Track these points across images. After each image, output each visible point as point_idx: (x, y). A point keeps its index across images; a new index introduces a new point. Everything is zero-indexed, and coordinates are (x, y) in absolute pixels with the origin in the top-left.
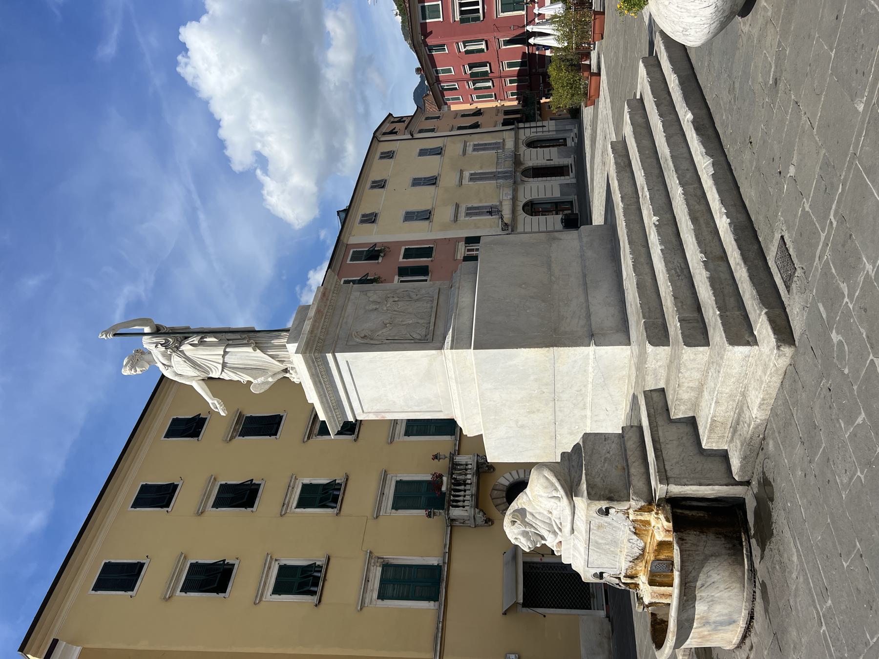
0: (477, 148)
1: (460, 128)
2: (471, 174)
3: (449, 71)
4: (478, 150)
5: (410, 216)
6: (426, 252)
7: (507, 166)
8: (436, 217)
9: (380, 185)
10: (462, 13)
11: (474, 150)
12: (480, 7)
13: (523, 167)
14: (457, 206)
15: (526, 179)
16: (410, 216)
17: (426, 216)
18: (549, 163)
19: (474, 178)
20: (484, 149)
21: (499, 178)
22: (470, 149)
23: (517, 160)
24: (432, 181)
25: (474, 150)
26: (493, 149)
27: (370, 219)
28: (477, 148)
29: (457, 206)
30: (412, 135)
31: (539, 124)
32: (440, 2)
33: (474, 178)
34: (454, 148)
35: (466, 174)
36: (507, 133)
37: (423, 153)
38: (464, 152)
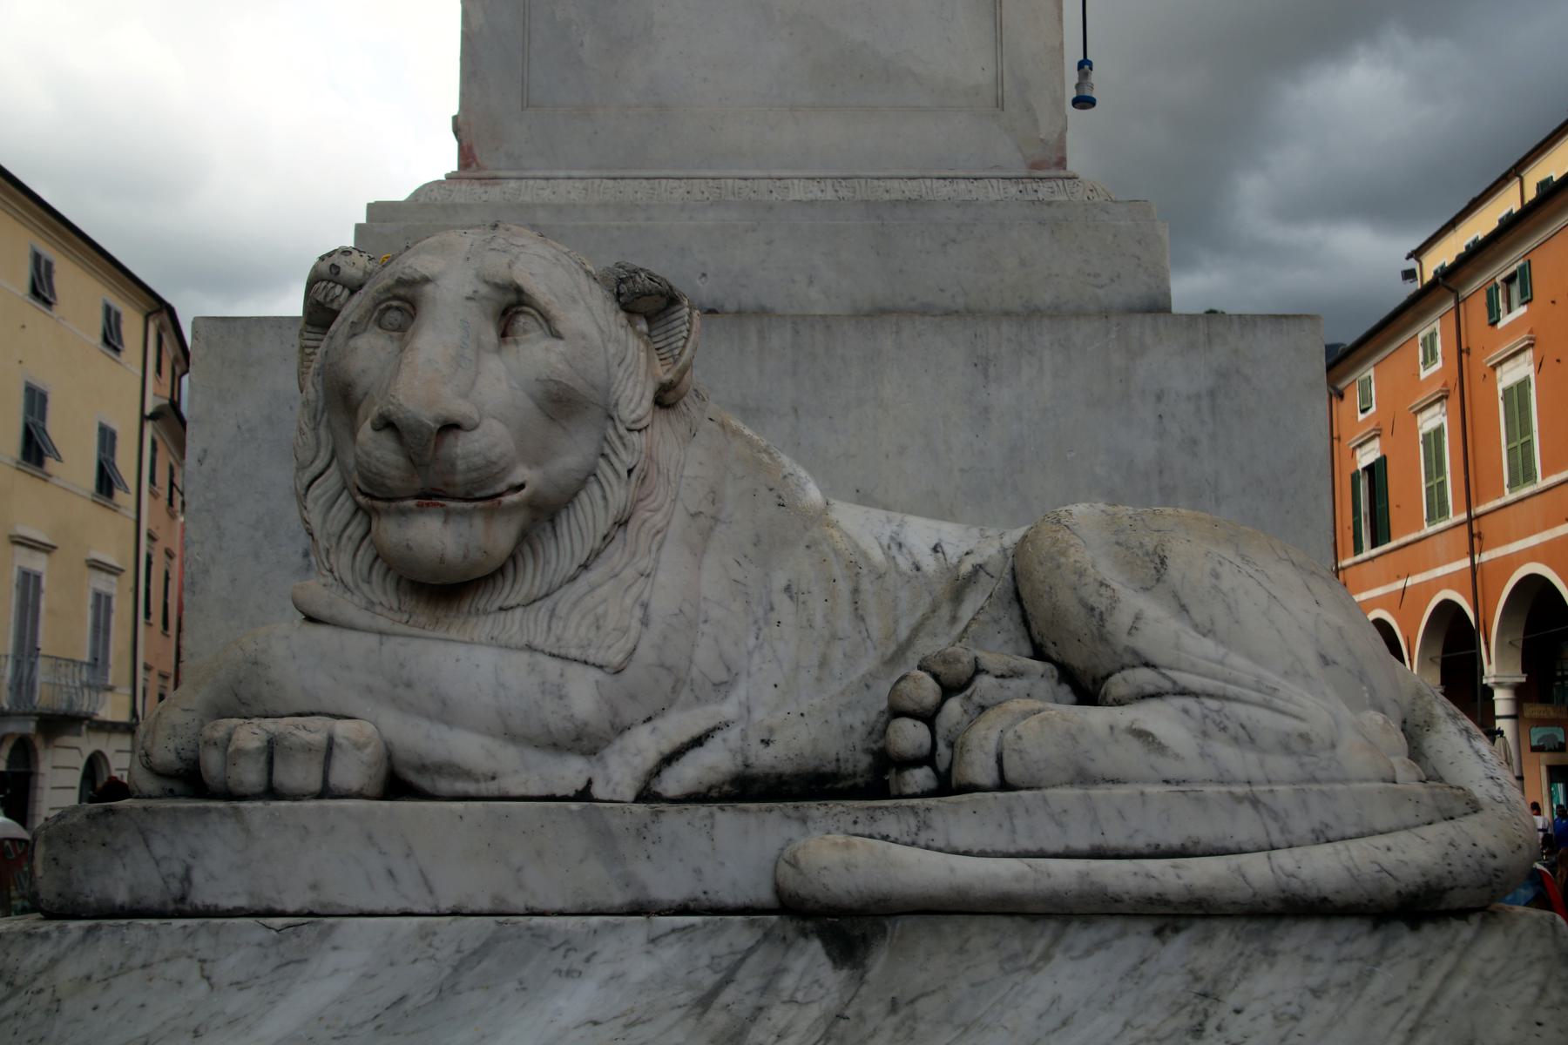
0: (102, 603)
1: (149, 557)
2: (38, 578)
4: (96, 606)
7: (46, 696)
9: (41, 290)
11: (98, 596)
13: (39, 742)
19: (29, 584)
21: (18, 664)
22: (102, 582)
23: (58, 724)
24: (35, 450)
25: (98, 596)
26: (94, 652)
28: (102, 603)
30: (154, 417)
33: (29, 584)
34: (109, 536)
35: (38, 563)
36: (126, 700)
37: (107, 438)
38: (96, 565)
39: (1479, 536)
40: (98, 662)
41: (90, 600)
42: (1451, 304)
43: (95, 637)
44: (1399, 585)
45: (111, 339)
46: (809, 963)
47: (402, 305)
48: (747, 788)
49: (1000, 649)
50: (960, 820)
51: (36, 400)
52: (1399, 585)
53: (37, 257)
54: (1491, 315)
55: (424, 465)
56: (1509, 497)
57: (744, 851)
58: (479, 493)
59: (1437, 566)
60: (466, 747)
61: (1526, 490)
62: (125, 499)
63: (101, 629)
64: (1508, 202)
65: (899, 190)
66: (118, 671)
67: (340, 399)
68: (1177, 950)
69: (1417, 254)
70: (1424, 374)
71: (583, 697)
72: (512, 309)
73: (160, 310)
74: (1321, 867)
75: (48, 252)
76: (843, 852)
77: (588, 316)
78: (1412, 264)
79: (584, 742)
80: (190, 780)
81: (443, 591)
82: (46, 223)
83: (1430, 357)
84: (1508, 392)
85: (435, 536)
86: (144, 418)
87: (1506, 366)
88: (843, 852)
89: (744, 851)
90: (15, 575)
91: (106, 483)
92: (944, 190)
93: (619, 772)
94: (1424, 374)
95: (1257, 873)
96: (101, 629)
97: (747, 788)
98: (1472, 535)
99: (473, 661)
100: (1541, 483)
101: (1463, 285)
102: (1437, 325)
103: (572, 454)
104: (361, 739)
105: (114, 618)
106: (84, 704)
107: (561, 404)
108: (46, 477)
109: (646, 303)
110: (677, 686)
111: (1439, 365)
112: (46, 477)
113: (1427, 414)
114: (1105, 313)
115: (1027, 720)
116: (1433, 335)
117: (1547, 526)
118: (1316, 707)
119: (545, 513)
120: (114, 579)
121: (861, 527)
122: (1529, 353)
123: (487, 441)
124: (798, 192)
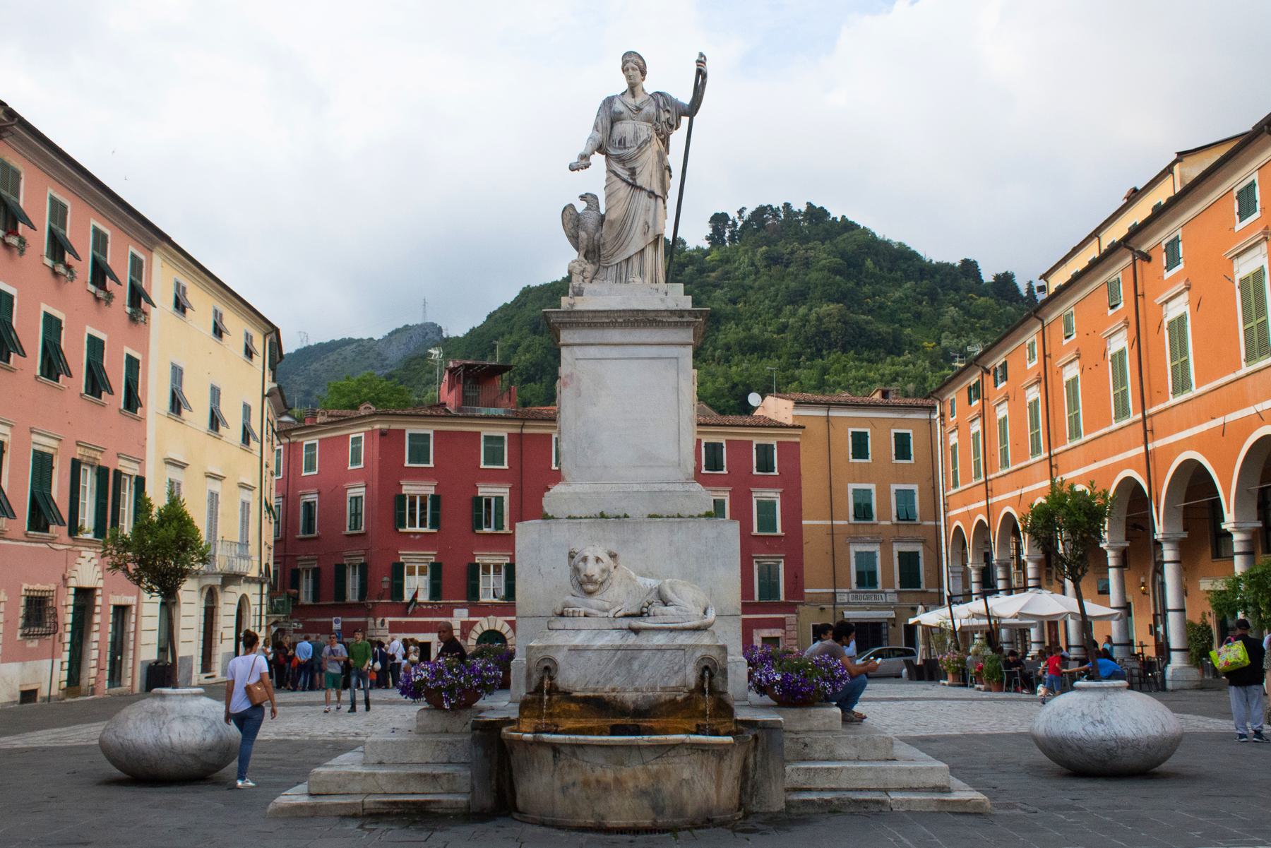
3: (310, 467)
4: (243, 510)
5: (177, 373)
6: (132, 401)
8: (171, 425)
10: (413, 499)
12: (418, 529)
13: (218, 590)
14: (182, 466)
15: (204, 595)
16: (177, 373)
17: (177, 404)
18: (219, 636)
19: (214, 497)
20: (243, 521)
24: (215, 422)
25: (243, 503)
27: (180, 306)
28: (245, 506)
29: (182, 466)
31: (264, 623)
32: (431, 465)
33: (214, 497)
35: (216, 486)
37: (247, 409)
38: (243, 486)
39: (1056, 466)
40: (244, 544)
41: (240, 507)
42: (1039, 327)
43: (242, 529)
44: (1018, 492)
45: (249, 353)
46: (633, 634)
47: (585, 559)
48: (626, 616)
49: (656, 599)
50: (649, 619)
51: (216, 393)
52: (1018, 492)
53: (216, 312)
54: (1111, 299)
55: (590, 579)
56: (1069, 445)
57: (625, 623)
58: (595, 582)
59: (1036, 482)
60: (593, 611)
61: (1076, 442)
62: (254, 445)
63: (245, 523)
64: (1092, 252)
65: (657, 487)
66: (253, 549)
67: (576, 570)
68: (672, 634)
69: (1045, 277)
70: (1029, 366)
71: (607, 606)
72: (598, 560)
73: (272, 332)
74: (687, 625)
75: (184, 281)
76: (636, 623)
77: (606, 559)
78: (1043, 283)
79: (607, 611)
80: (562, 615)
81: (590, 593)
82: (184, 264)
83: (1032, 356)
84: (1068, 383)
85: (590, 587)
86: (264, 396)
87: (1067, 368)
88: (636, 623)
89: (625, 623)
90: (207, 494)
91: (247, 436)
92: (666, 487)
93: (611, 615)
94: (1029, 366)
95: (680, 625)
96: (245, 523)
97: (626, 616)
98: (1051, 466)
99: (593, 601)
100: (1084, 438)
101: (1047, 316)
102: (1035, 337)
103: (605, 576)
104: (583, 610)
105: (251, 515)
106: (240, 566)
107: (603, 571)
108: (220, 438)
109: (613, 556)
110: (617, 603)
111: (1035, 362)
112: (220, 438)
113: (1031, 390)
114: (699, 516)
115: (658, 608)
116: (1033, 343)
117: (1087, 464)
118: (691, 607)
119: (602, 583)
120: (218, 483)
121: (640, 581)
122: (1077, 362)
123: (597, 576)
124: (636, 488)
